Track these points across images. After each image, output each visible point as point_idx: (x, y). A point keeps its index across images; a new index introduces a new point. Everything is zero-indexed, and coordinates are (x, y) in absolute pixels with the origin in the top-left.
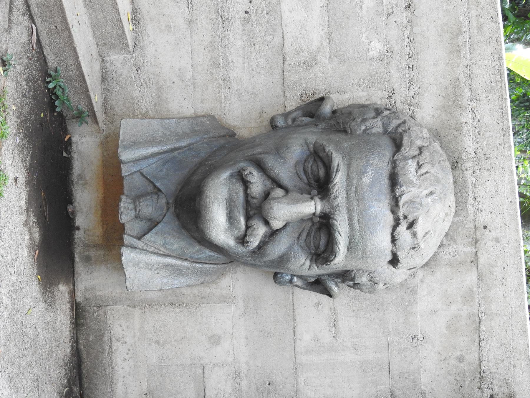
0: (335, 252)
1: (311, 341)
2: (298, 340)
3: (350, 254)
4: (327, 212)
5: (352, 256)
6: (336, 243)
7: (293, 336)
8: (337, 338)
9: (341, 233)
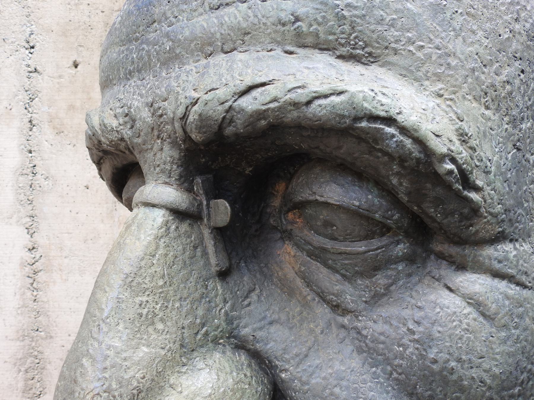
0: (357, 119)
3: (396, 52)
4: (176, 154)
5: (411, 42)
6: (296, 105)
9: (249, 81)
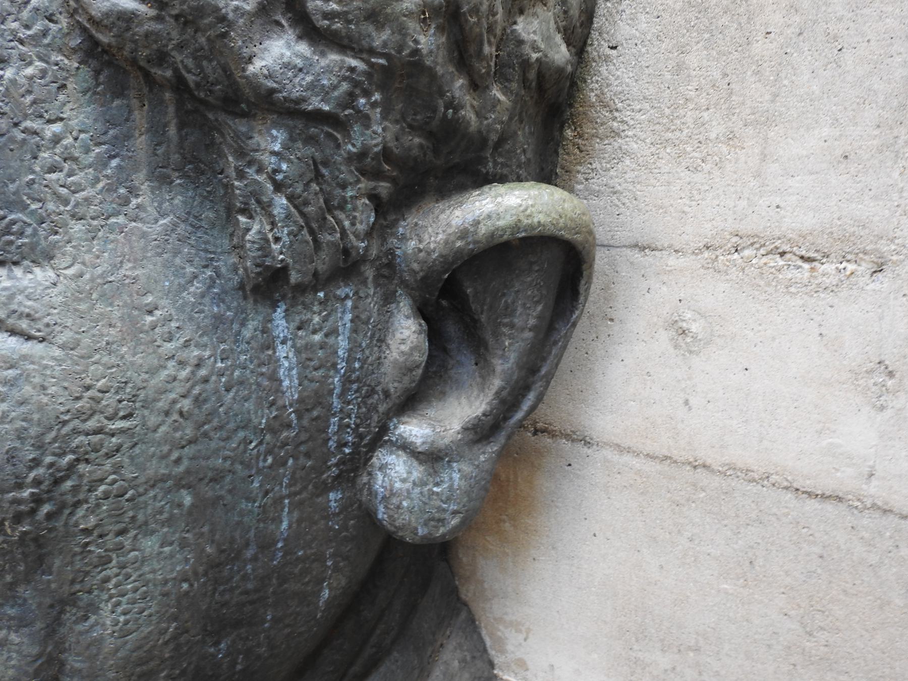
1: (888, 413)
2: (874, 490)
7: (842, 507)
8: (885, 247)
